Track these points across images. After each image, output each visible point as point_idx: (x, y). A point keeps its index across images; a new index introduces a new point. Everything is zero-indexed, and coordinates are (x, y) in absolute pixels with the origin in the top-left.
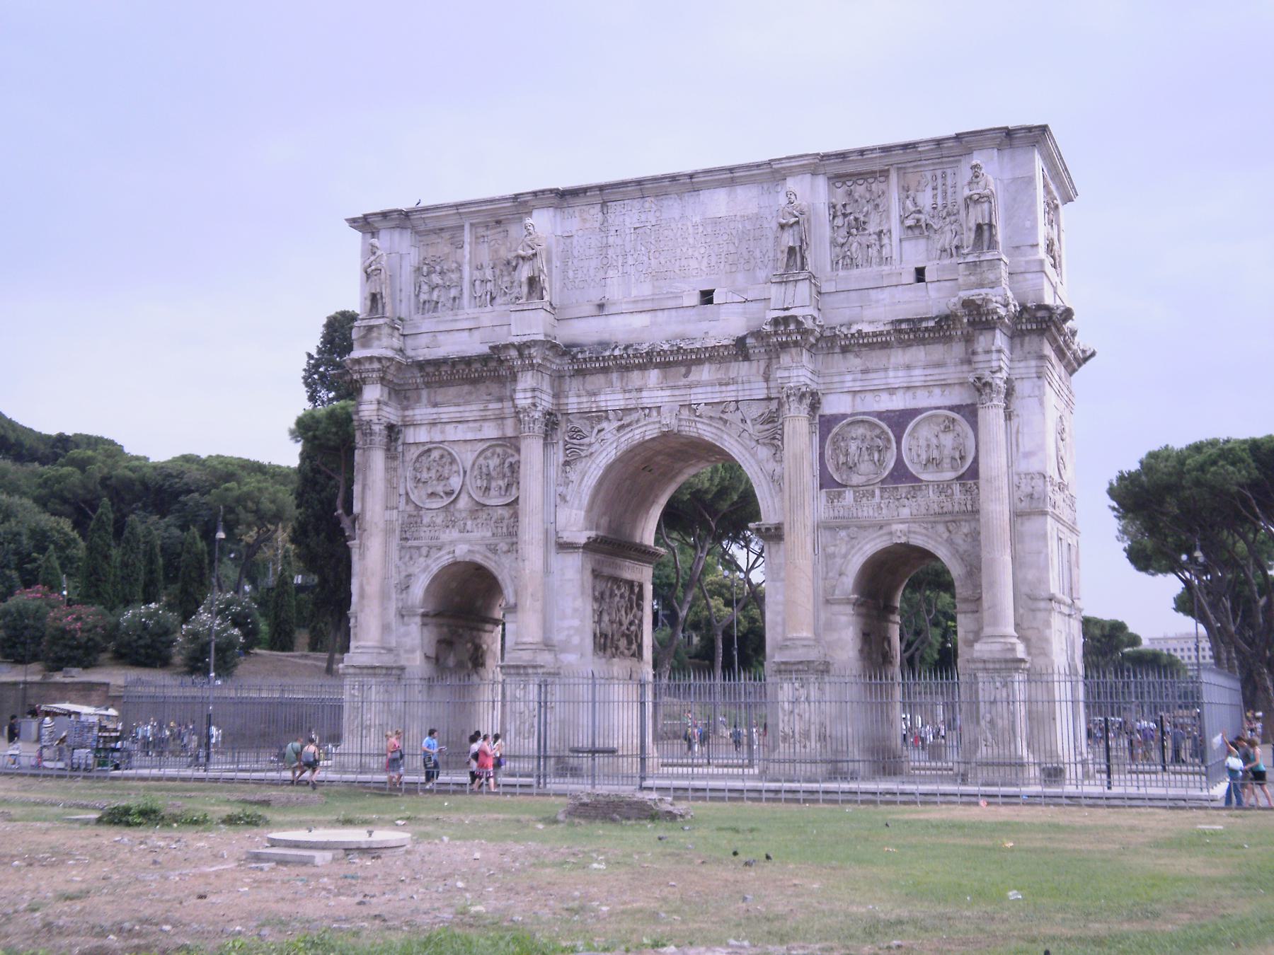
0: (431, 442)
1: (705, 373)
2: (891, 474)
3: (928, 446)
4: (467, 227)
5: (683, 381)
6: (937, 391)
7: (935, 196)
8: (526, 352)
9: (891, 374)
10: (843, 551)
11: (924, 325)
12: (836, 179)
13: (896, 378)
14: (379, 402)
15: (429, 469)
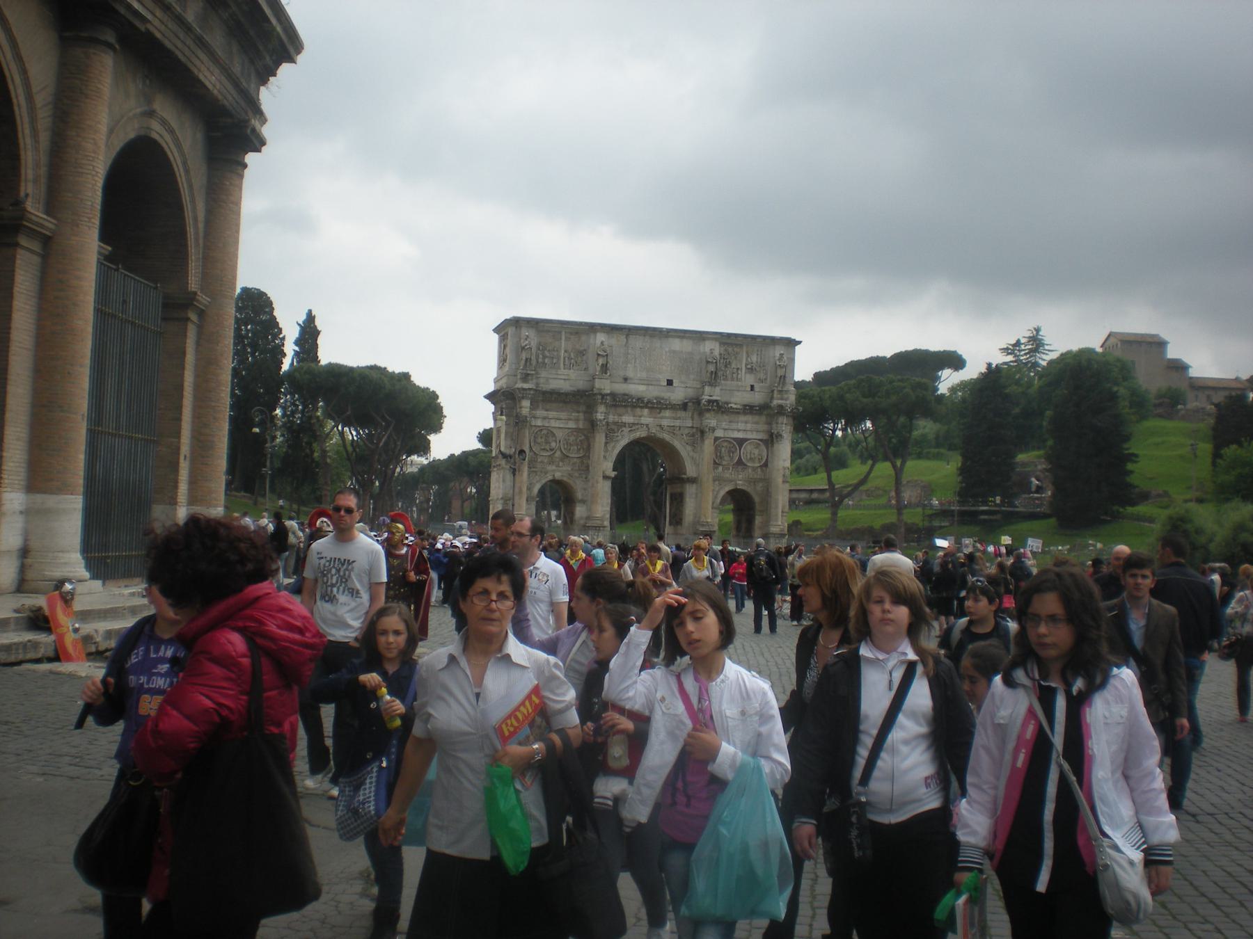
0: (543, 426)
1: (667, 413)
2: (737, 462)
3: (751, 453)
4: (563, 333)
5: (659, 416)
6: (755, 433)
7: (757, 358)
8: (605, 397)
9: (739, 424)
10: (717, 489)
11: (755, 408)
12: (722, 344)
13: (741, 426)
14: (530, 408)
15: (541, 438)
